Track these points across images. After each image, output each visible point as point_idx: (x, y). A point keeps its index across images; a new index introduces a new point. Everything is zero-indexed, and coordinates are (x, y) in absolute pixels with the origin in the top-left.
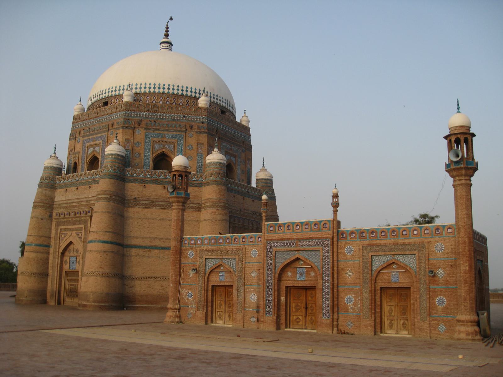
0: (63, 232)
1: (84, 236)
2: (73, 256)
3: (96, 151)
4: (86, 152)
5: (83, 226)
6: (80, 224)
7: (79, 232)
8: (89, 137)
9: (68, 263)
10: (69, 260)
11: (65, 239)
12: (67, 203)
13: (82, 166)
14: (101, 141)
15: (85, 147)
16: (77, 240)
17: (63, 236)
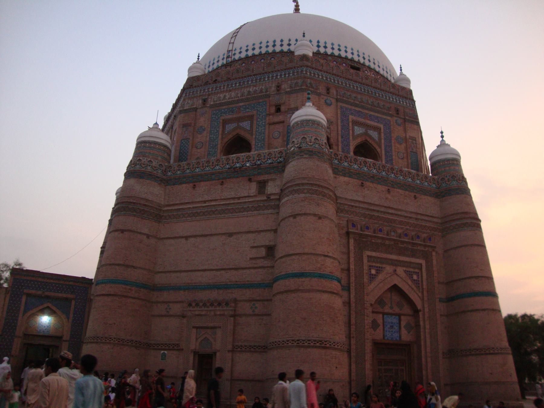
0: (374, 264)
1: (427, 279)
2: (392, 314)
3: (371, 137)
4: (351, 128)
5: (423, 262)
6: (413, 256)
7: (412, 270)
8: (353, 108)
9: (381, 327)
10: (381, 321)
11: (380, 277)
12: (374, 210)
13: (343, 149)
14: (382, 126)
15: (348, 119)
16: (409, 285)
17: (373, 272)
